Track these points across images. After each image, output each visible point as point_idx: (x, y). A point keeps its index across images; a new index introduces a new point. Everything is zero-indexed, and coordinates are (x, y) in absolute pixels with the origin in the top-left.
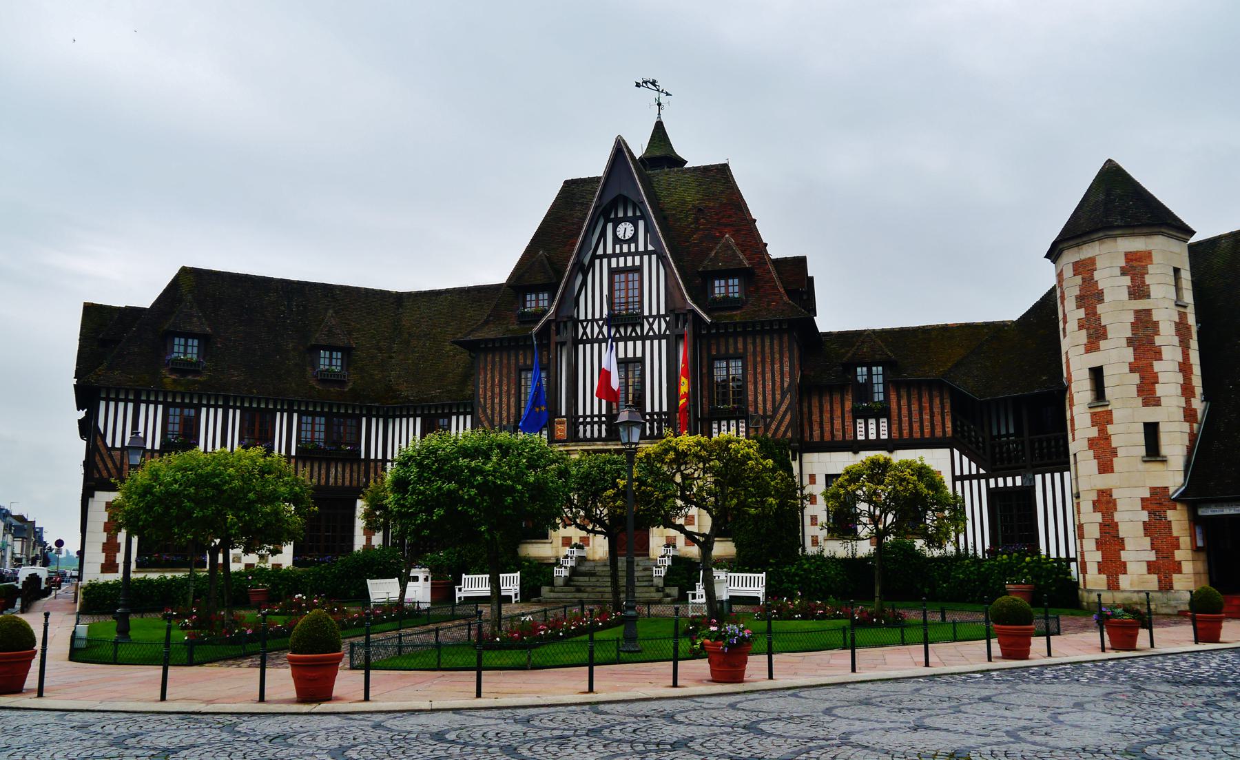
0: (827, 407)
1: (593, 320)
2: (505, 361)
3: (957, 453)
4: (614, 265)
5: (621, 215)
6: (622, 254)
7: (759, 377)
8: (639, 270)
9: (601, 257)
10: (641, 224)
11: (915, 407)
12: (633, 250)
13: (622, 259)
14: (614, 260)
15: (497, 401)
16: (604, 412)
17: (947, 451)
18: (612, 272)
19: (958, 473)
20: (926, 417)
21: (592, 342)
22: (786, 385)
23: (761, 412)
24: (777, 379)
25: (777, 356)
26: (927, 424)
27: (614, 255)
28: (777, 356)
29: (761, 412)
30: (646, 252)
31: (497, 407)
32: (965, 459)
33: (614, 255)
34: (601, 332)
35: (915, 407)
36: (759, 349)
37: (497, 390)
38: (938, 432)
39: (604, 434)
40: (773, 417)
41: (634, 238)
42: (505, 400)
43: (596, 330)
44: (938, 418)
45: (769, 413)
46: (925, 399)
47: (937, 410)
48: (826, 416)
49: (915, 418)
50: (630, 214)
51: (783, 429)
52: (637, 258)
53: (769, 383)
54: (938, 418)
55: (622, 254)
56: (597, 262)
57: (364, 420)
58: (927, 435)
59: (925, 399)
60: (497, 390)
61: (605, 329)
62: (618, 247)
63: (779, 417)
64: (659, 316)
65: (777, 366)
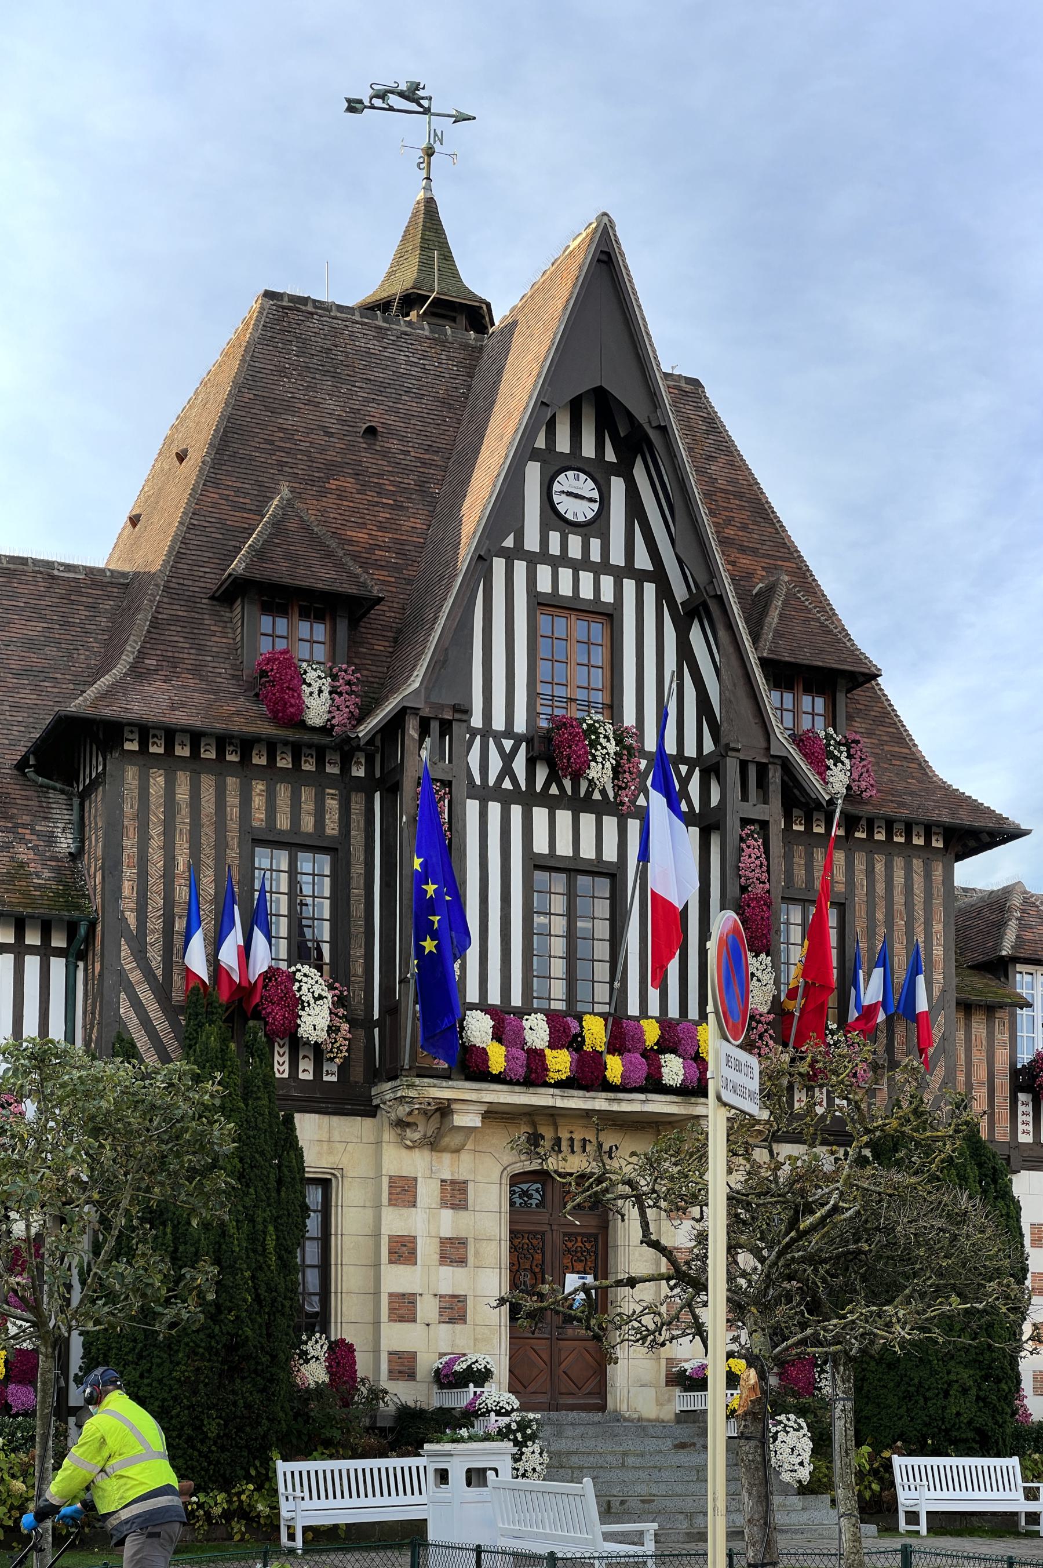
1: (487, 732)
4: (544, 586)
8: (611, 616)
9: (510, 556)
12: (595, 556)
14: (544, 572)
18: (539, 603)
21: (484, 794)
27: (543, 556)
33: (543, 556)
34: (507, 770)
43: (495, 764)
52: (607, 582)
56: (499, 565)
61: (519, 765)
62: (554, 537)
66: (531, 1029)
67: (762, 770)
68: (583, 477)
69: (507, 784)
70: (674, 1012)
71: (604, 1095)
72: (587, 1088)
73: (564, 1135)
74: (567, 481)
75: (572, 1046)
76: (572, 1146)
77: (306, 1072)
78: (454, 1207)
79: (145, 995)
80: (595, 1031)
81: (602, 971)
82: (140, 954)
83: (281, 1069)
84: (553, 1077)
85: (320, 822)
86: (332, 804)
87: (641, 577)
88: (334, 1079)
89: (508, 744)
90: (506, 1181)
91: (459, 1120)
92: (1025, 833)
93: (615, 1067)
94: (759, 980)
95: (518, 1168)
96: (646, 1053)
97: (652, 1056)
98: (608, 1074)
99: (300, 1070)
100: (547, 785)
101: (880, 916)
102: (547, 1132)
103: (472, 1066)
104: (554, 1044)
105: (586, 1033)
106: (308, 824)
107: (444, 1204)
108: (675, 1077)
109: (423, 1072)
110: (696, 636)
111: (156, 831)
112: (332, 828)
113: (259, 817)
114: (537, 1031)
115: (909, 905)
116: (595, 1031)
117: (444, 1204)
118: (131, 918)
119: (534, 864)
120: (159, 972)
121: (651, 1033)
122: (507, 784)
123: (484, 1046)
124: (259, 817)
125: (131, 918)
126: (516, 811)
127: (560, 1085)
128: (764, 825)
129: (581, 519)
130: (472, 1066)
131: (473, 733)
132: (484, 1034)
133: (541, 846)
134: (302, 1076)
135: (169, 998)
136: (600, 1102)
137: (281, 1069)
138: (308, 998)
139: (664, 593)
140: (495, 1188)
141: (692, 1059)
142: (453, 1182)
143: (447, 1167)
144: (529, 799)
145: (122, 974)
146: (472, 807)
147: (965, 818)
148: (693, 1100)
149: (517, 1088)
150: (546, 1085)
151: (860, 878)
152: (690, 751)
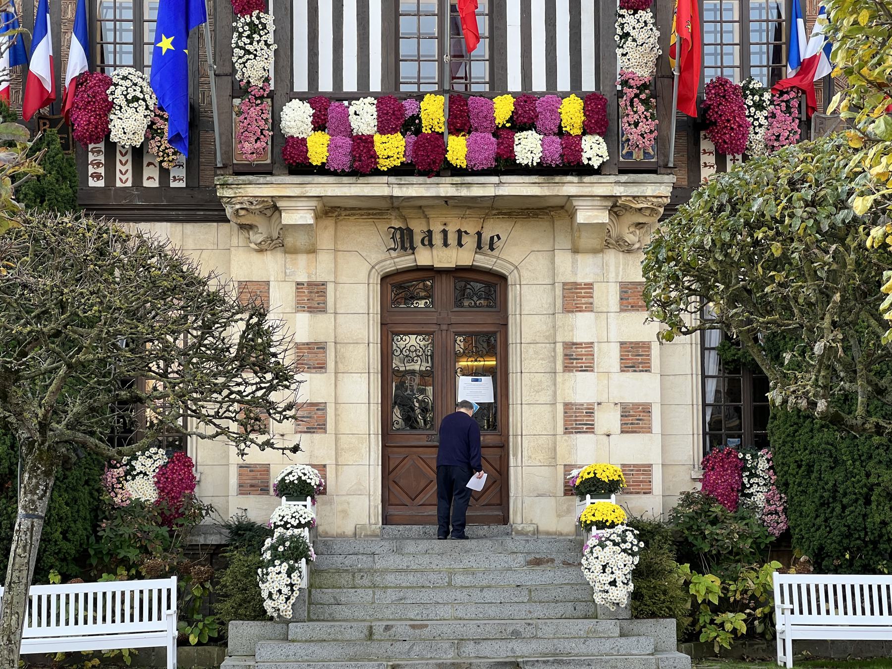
66: (356, 114)
70: (539, 84)
71: (449, 180)
72: (427, 173)
73: (437, 228)
75: (410, 130)
77: (124, 178)
78: (312, 310)
80: (433, 112)
81: (483, 48)
83: (124, 178)
84: (384, 164)
88: (182, 184)
90: (376, 280)
91: (288, 218)
93: (457, 149)
94: (634, 40)
95: (390, 266)
96: (497, 132)
97: (504, 135)
98: (449, 156)
99: (145, 178)
102: (418, 228)
103: (293, 160)
104: (383, 129)
105: (423, 115)
107: (300, 307)
108: (530, 155)
109: (242, 169)
114: (364, 117)
116: (433, 112)
117: (300, 307)
121: (503, 109)
123: (305, 136)
127: (394, 172)
130: (293, 160)
132: (300, 124)
134: (146, 184)
136: (445, 187)
137: (124, 178)
138: (120, 100)
140: (363, 288)
141: (555, 134)
142: (310, 284)
143: (303, 269)
148: (557, 179)
149: (345, 179)
150: (378, 173)
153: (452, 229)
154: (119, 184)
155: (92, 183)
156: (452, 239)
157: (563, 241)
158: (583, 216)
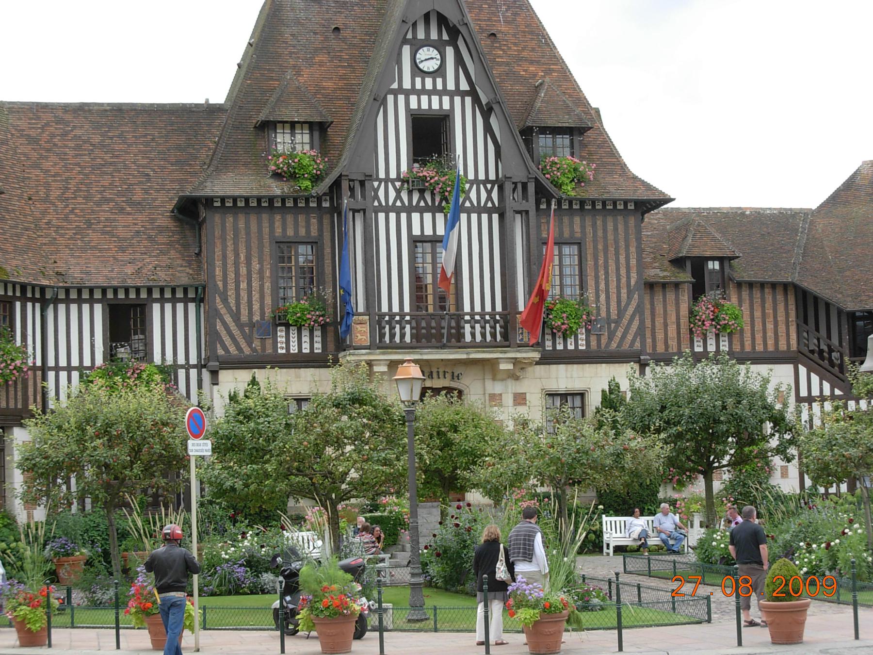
0: (659, 308)
1: (387, 180)
2: (254, 227)
3: (803, 370)
4: (414, 105)
5: (421, 35)
6: (424, 91)
7: (602, 273)
9: (396, 93)
10: (450, 51)
11: (758, 314)
12: (439, 86)
13: (424, 99)
14: (413, 99)
15: (243, 285)
16: (407, 309)
17: (790, 367)
19: (804, 393)
20: (770, 326)
21: (387, 210)
22: (633, 282)
23: (603, 314)
24: (623, 272)
25: (622, 244)
26: (770, 334)
28: (622, 244)
29: (603, 314)
30: (458, 92)
31: (244, 295)
32: (815, 378)
33: (413, 91)
35: (758, 314)
36: (600, 233)
37: (243, 270)
38: (783, 346)
39: (408, 339)
40: (617, 322)
41: (440, 72)
42: (255, 284)
43: (392, 194)
44: (782, 328)
45: (614, 316)
46: (769, 304)
47: (781, 318)
48: (659, 321)
49: (758, 326)
50: (434, 36)
51: (630, 337)
52: (446, 99)
53: (613, 278)
54: (782, 328)
55: (424, 91)
57: (18, 305)
58: (771, 348)
59: (769, 304)
60: (243, 270)
62: (418, 80)
63: (625, 321)
64: (487, 180)
65: (622, 259)
67: (525, 186)
68: (431, 49)
69: (398, 204)
74: (423, 53)
76: (438, 375)
79: (228, 319)
82: (225, 300)
85: (308, 231)
86: (314, 221)
87: (463, 94)
89: (398, 184)
92: (673, 200)
100: (419, 202)
101: (600, 247)
106: (302, 232)
110: (493, 121)
111: (230, 243)
112: (314, 232)
113: (278, 231)
115: (616, 242)
118: (220, 284)
119: (414, 242)
120: (234, 308)
122: (398, 204)
124: (278, 231)
125: (220, 284)
126: (404, 216)
128: (527, 212)
129: (431, 70)
131: (380, 181)
133: (416, 232)
134: (304, 351)
135: (239, 319)
139: (476, 100)
144: (409, 210)
145: (216, 310)
146: (382, 216)
147: (642, 195)
151: (589, 229)
152: (492, 177)
153: (441, 371)
154: (292, 351)
155: (280, 351)
156: (441, 375)
157: (488, 376)
158: (503, 366)
